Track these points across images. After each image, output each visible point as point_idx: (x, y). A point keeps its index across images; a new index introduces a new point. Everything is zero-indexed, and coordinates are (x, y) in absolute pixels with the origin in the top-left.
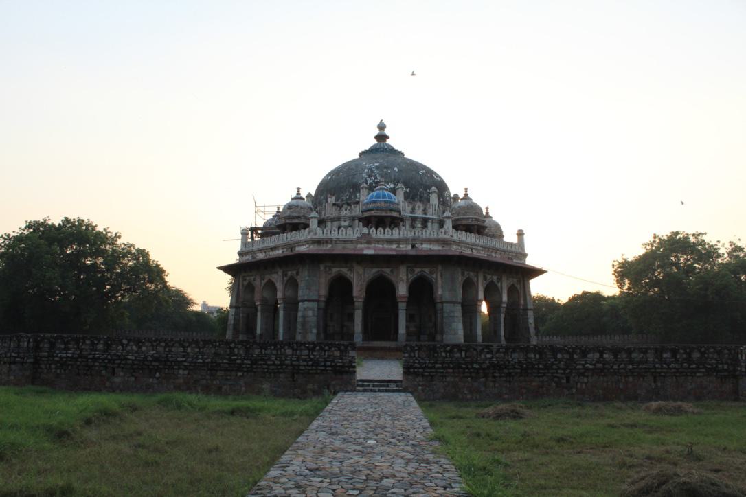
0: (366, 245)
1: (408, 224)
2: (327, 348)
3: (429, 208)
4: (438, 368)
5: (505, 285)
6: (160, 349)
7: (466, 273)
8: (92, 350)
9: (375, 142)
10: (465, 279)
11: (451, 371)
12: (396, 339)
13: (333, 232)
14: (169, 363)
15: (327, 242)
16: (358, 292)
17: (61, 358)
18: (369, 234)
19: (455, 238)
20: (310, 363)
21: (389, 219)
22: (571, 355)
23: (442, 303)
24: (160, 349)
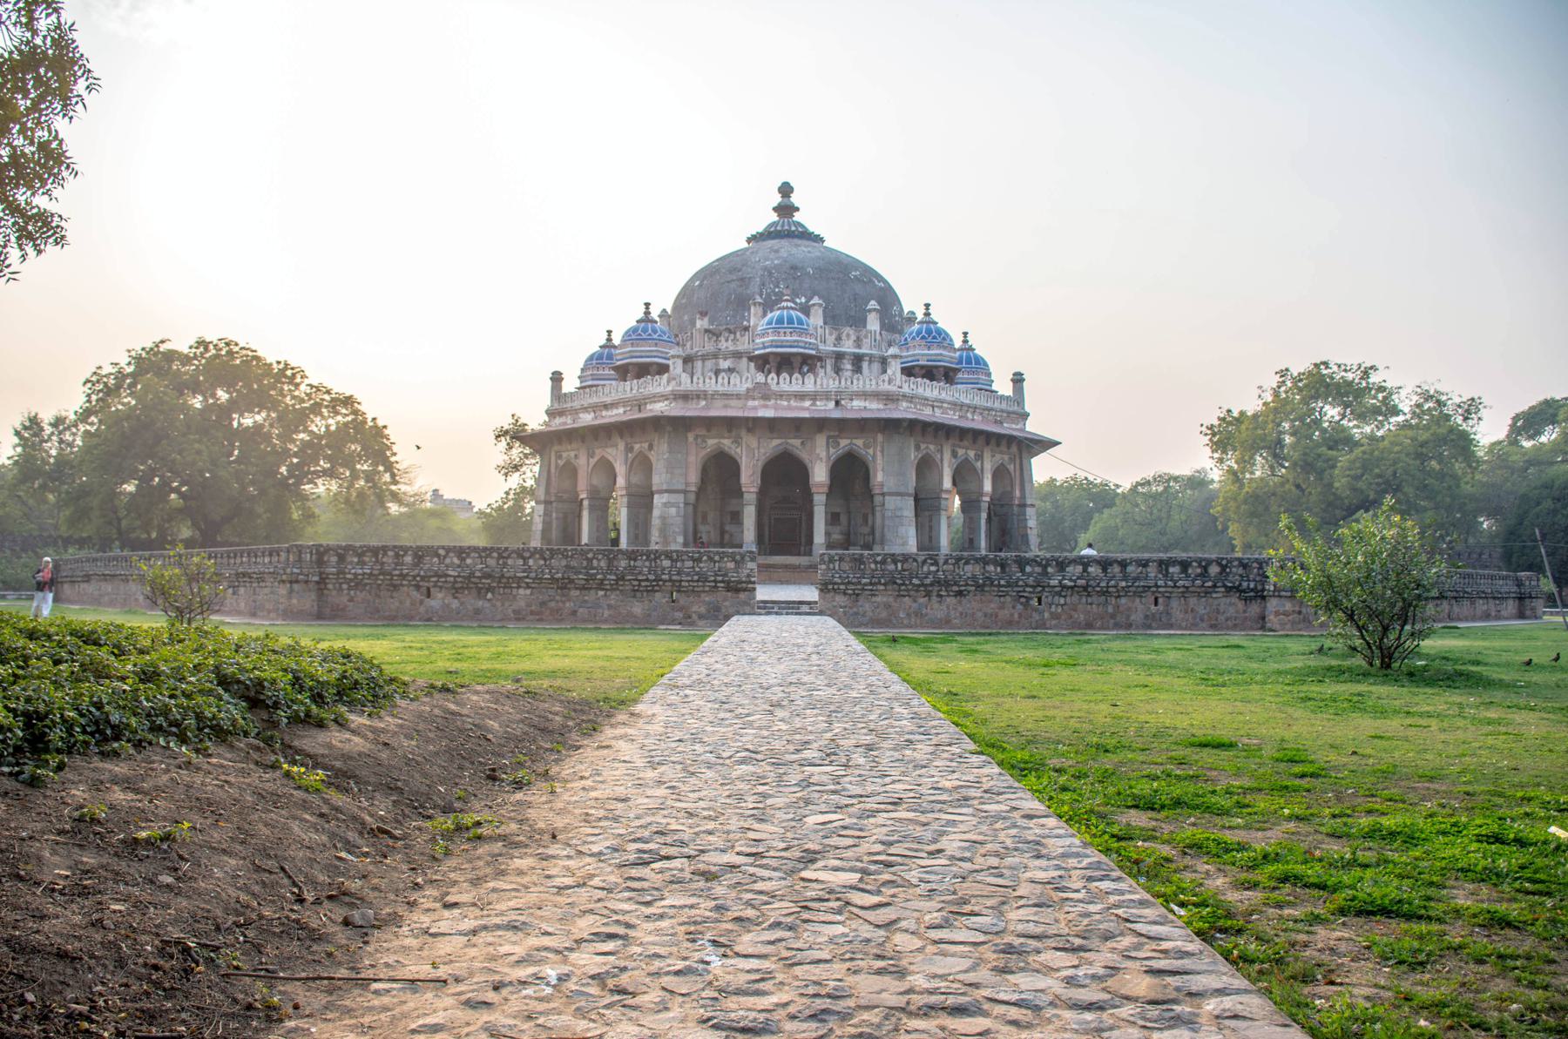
0: (762, 402)
1: (829, 364)
2: (717, 558)
3: (866, 337)
4: (865, 584)
5: (988, 466)
6: (492, 562)
7: (923, 446)
8: (397, 564)
9: (774, 217)
11: (882, 587)
12: (809, 553)
13: (707, 380)
14: (504, 580)
15: (698, 397)
16: (749, 479)
17: (355, 574)
18: (766, 384)
19: (906, 389)
20: (696, 578)
21: (799, 359)
22: (1045, 567)
23: (883, 494)
24: (492, 562)
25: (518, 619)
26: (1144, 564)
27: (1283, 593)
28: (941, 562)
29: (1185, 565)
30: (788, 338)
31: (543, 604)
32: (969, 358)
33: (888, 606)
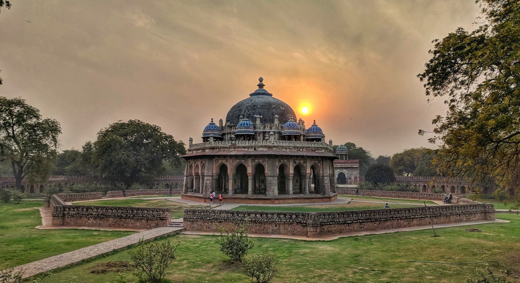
0: (234, 149)
2: (158, 211)
3: (273, 126)
4: (195, 219)
6: (104, 211)
7: (282, 161)
9: (258, 88)
10: (281, 164)
11: (199, 220)
15: (216, 148)
16: (231, 172)
17: (72, 214)
19: (276, 144)
20: (152, 216)
22: (244, 215)
24: (104, 211)
25: (110, 227)
26: (273, 214)
27: (310, 225)
28: (216, 213)
29: (285, 215)
30: (243, 130)
31: (116, 222)
32: (316, 128)
33: (201, 225)
